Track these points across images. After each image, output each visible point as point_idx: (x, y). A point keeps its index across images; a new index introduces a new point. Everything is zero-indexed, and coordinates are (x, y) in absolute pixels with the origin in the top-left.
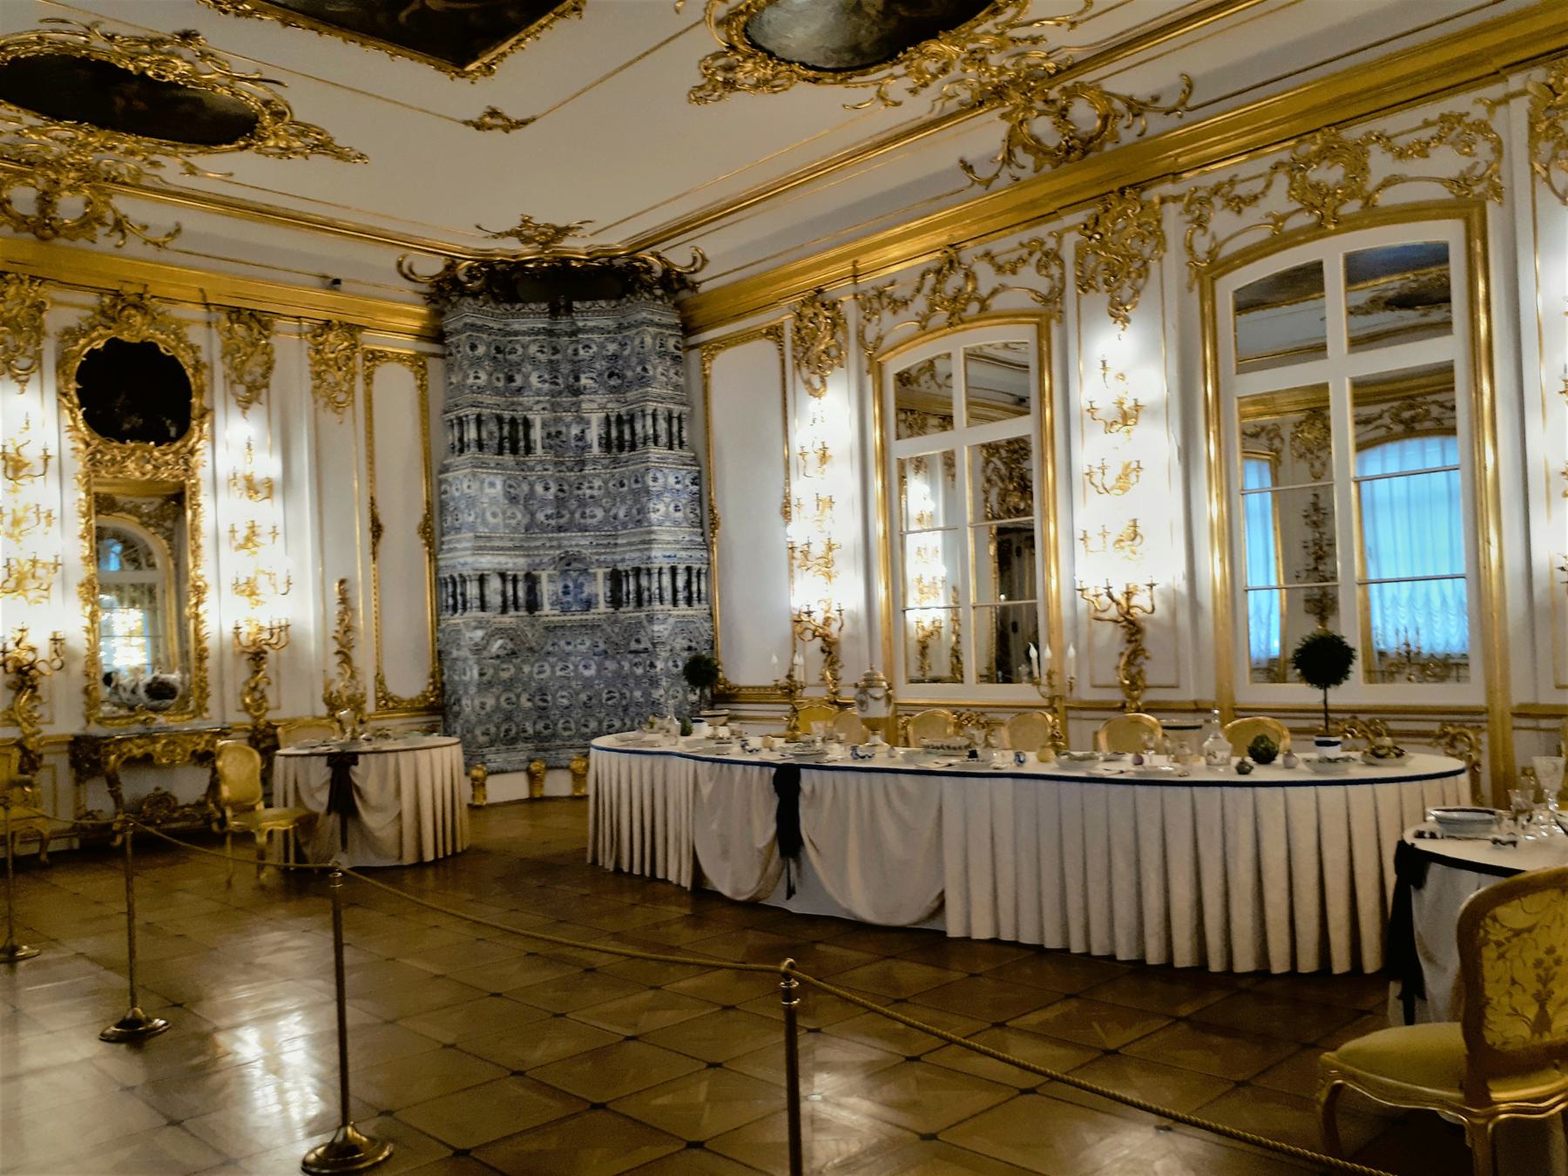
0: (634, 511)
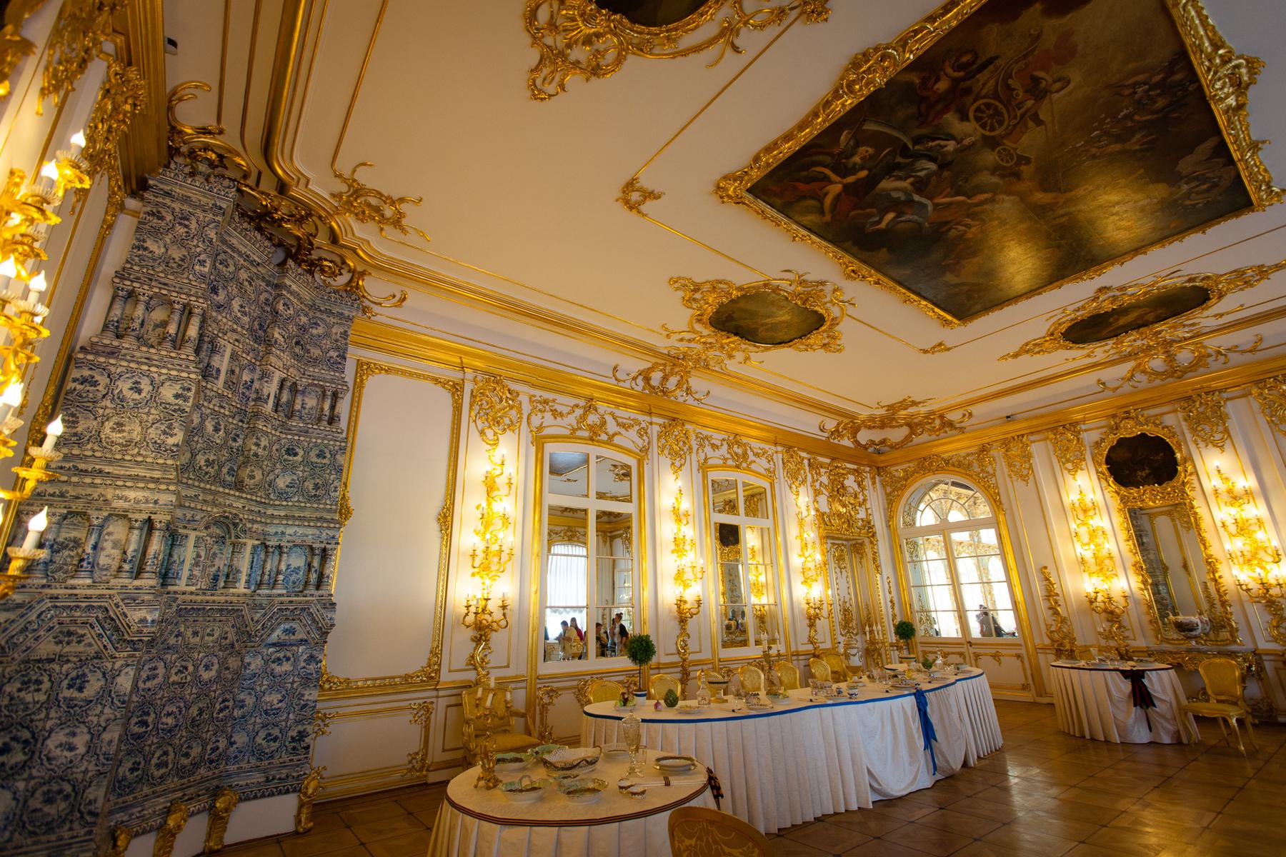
0: (309, 485)
